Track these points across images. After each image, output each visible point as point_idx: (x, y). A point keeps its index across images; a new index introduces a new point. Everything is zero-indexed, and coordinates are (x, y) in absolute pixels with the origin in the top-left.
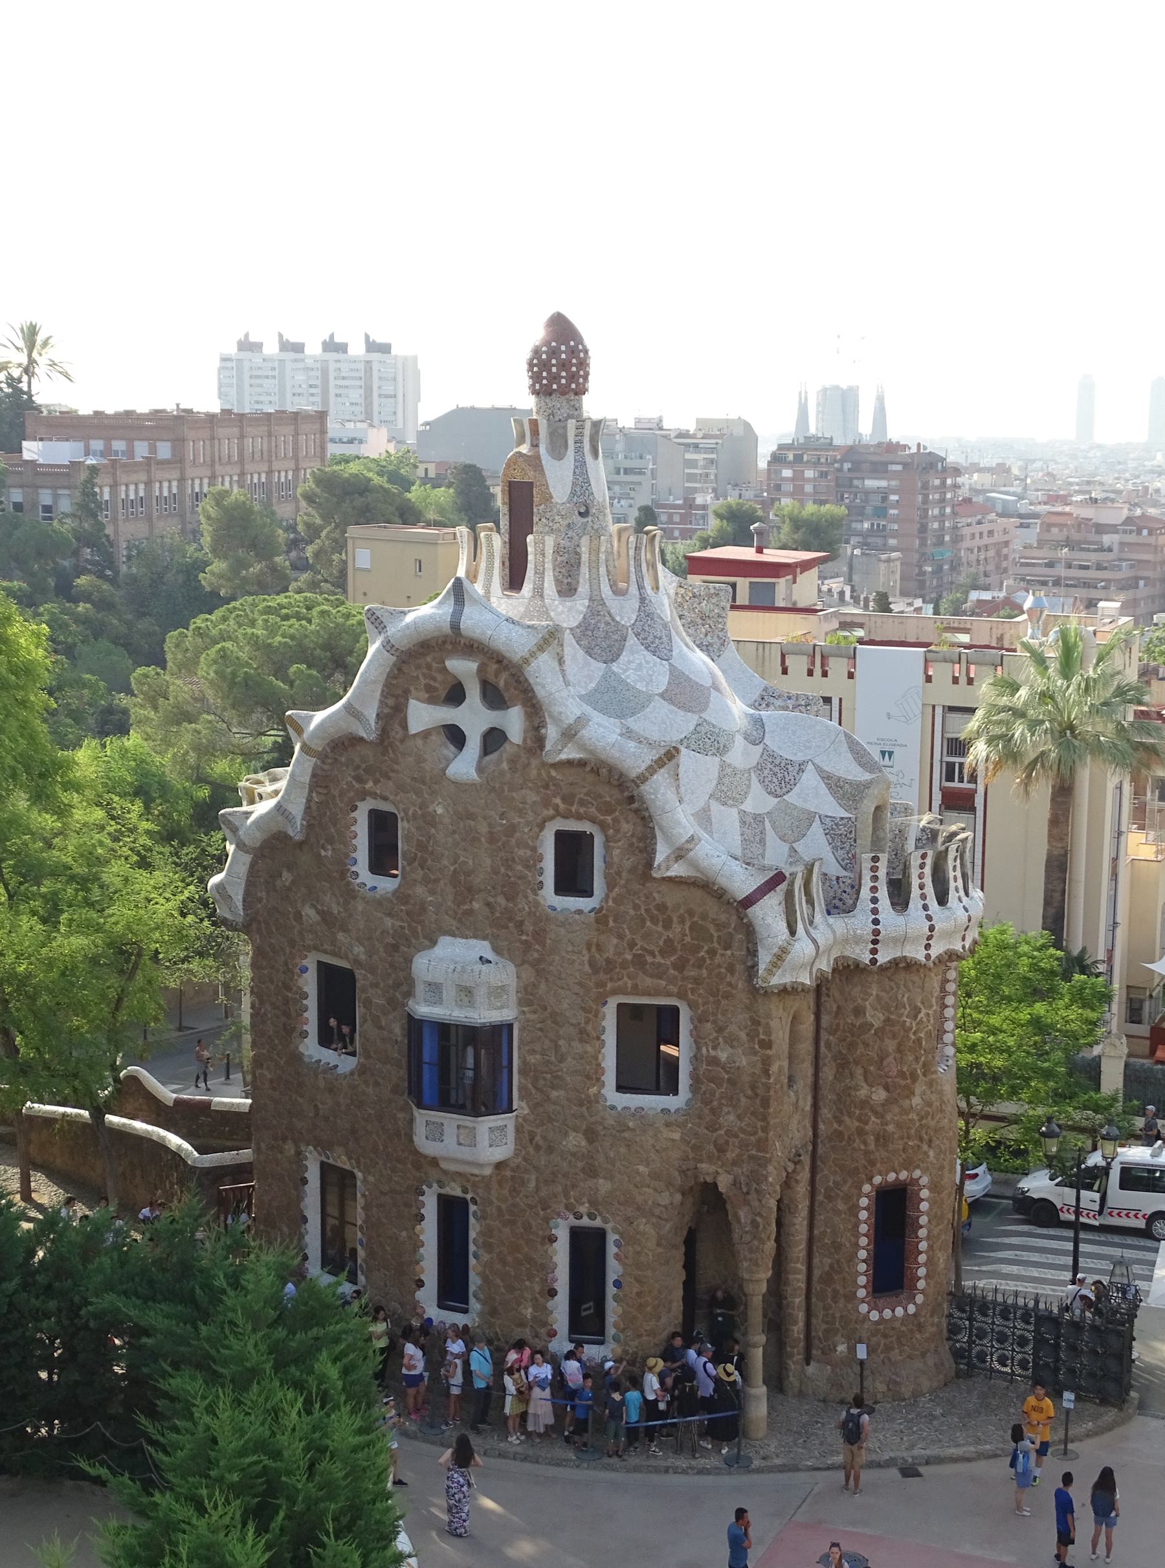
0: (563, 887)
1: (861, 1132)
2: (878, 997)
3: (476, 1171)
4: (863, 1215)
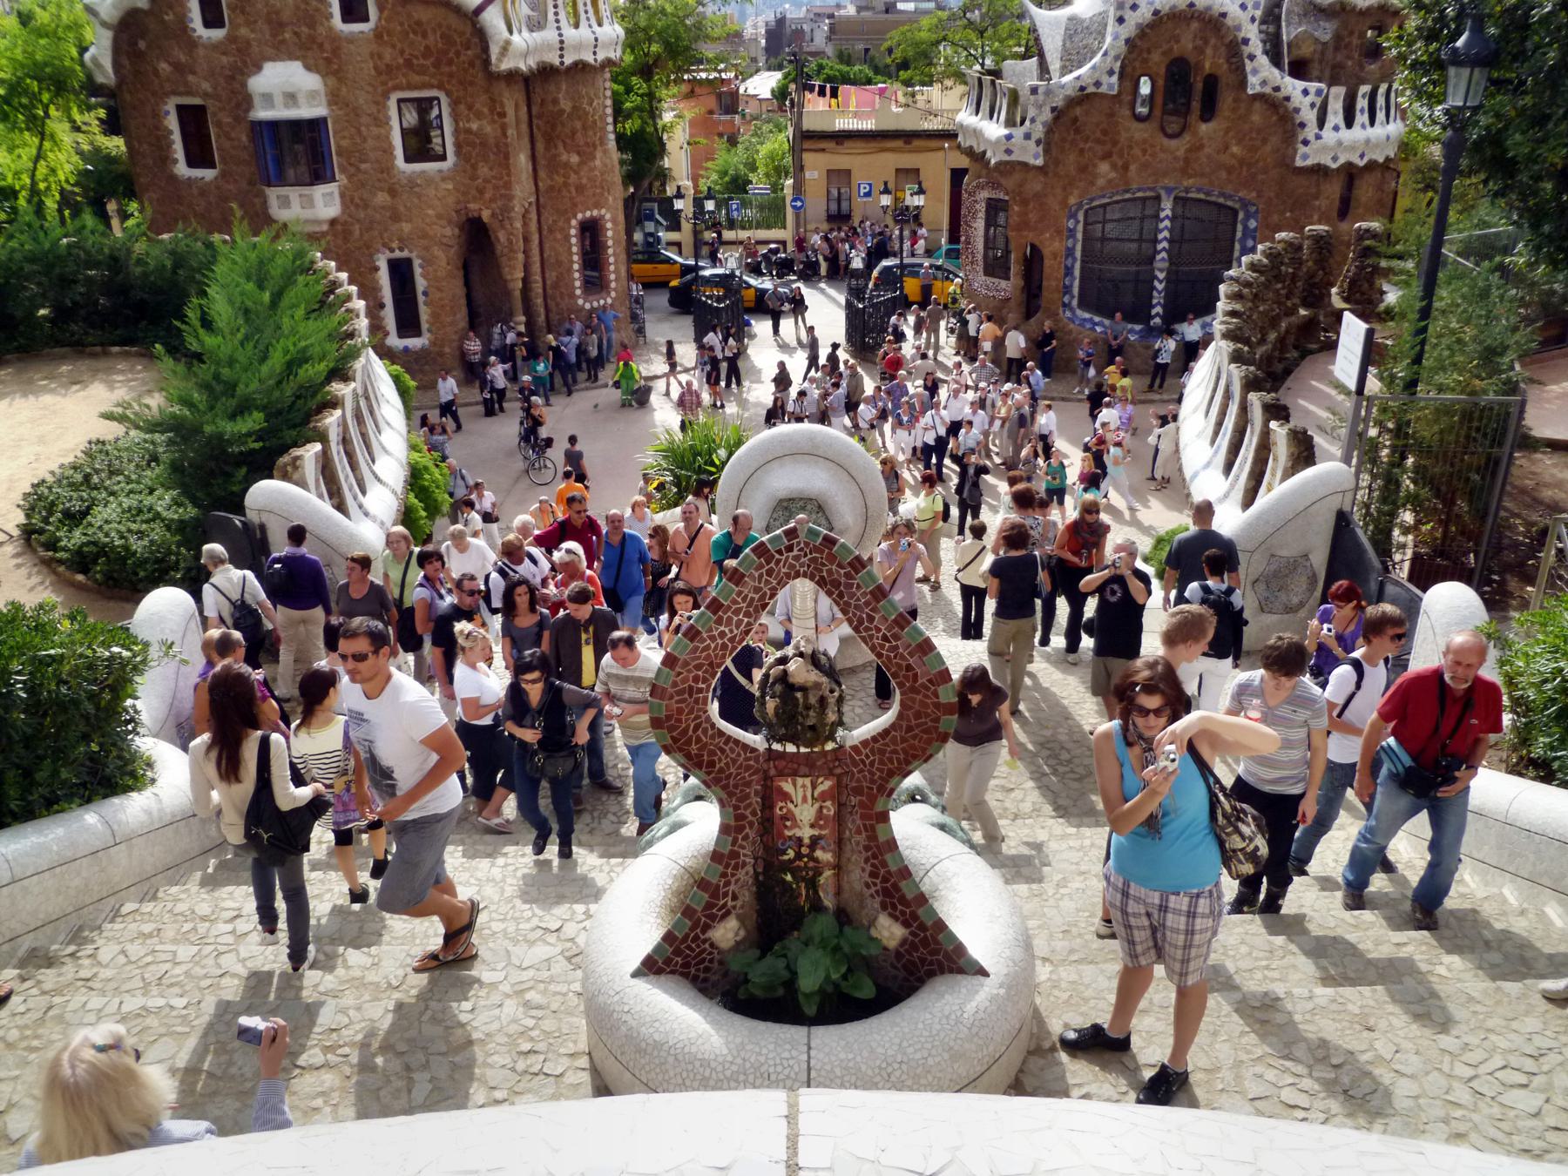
1: (566, 184)
2: (567, 92)
3: (317, 229)
4: (574, 240)
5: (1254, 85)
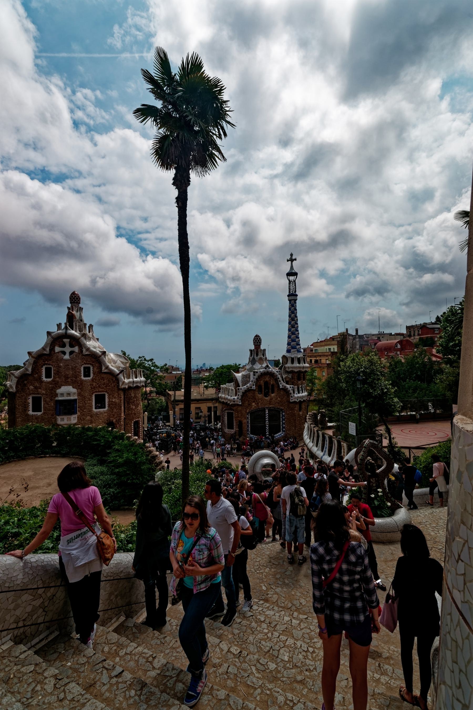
0: (84, 377)
1: (132, 413)
5: (281, 387)
